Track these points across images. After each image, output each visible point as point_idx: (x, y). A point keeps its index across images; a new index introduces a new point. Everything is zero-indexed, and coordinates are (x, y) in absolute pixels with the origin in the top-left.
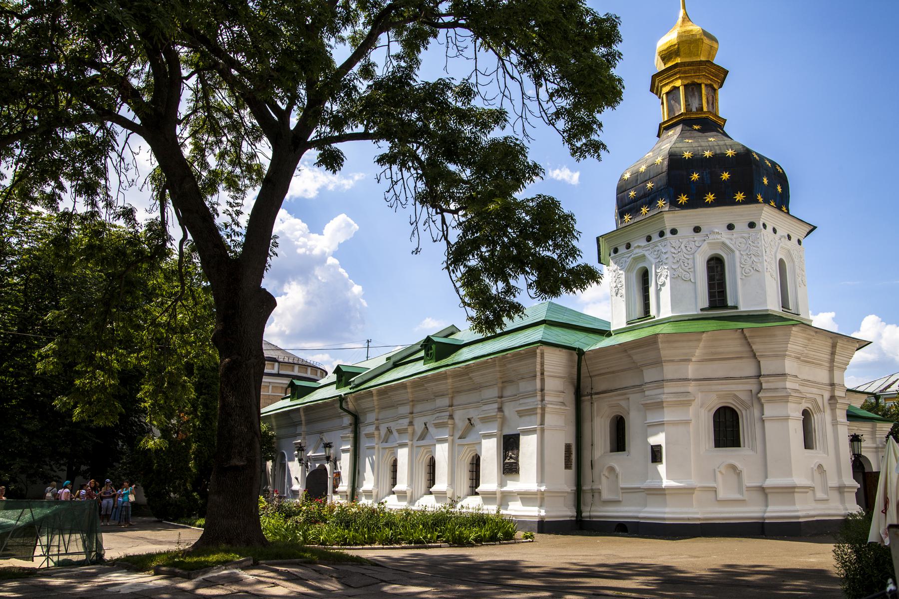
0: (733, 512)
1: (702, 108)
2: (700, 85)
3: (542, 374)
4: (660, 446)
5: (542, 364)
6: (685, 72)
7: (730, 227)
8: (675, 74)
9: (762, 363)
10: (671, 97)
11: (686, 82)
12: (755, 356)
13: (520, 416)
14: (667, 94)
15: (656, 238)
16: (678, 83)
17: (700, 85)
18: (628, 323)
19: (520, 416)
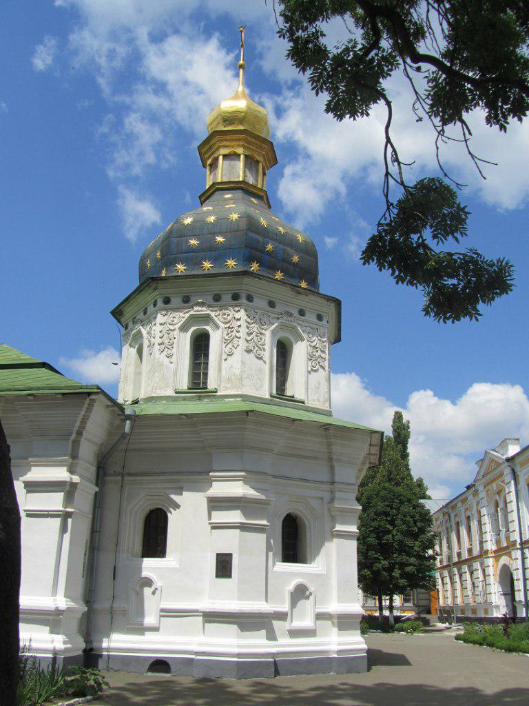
0: (303, 645)
1: (257, 185)
2: (258, 162)
3: (80, 433)
4: (230, 555)
5: (84, 421)
6: (248, 142)
7: (302, 313)
8: (239, 140)
9: (336, 468)
10: (227, 163)
11: (248, 153)
12: (330, 459)
13: (28, 492)
14: (225, 156)
15: (227, 298)
16: (240, 151)
17: (258, 162)
18: (189, 389)
19: (28, 492)
